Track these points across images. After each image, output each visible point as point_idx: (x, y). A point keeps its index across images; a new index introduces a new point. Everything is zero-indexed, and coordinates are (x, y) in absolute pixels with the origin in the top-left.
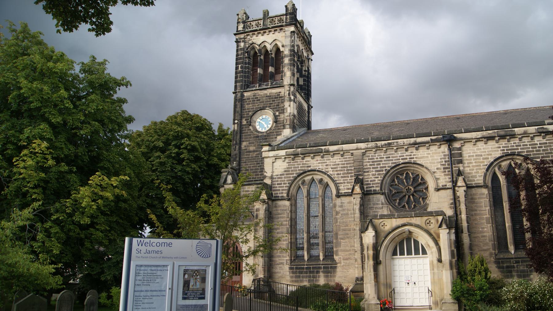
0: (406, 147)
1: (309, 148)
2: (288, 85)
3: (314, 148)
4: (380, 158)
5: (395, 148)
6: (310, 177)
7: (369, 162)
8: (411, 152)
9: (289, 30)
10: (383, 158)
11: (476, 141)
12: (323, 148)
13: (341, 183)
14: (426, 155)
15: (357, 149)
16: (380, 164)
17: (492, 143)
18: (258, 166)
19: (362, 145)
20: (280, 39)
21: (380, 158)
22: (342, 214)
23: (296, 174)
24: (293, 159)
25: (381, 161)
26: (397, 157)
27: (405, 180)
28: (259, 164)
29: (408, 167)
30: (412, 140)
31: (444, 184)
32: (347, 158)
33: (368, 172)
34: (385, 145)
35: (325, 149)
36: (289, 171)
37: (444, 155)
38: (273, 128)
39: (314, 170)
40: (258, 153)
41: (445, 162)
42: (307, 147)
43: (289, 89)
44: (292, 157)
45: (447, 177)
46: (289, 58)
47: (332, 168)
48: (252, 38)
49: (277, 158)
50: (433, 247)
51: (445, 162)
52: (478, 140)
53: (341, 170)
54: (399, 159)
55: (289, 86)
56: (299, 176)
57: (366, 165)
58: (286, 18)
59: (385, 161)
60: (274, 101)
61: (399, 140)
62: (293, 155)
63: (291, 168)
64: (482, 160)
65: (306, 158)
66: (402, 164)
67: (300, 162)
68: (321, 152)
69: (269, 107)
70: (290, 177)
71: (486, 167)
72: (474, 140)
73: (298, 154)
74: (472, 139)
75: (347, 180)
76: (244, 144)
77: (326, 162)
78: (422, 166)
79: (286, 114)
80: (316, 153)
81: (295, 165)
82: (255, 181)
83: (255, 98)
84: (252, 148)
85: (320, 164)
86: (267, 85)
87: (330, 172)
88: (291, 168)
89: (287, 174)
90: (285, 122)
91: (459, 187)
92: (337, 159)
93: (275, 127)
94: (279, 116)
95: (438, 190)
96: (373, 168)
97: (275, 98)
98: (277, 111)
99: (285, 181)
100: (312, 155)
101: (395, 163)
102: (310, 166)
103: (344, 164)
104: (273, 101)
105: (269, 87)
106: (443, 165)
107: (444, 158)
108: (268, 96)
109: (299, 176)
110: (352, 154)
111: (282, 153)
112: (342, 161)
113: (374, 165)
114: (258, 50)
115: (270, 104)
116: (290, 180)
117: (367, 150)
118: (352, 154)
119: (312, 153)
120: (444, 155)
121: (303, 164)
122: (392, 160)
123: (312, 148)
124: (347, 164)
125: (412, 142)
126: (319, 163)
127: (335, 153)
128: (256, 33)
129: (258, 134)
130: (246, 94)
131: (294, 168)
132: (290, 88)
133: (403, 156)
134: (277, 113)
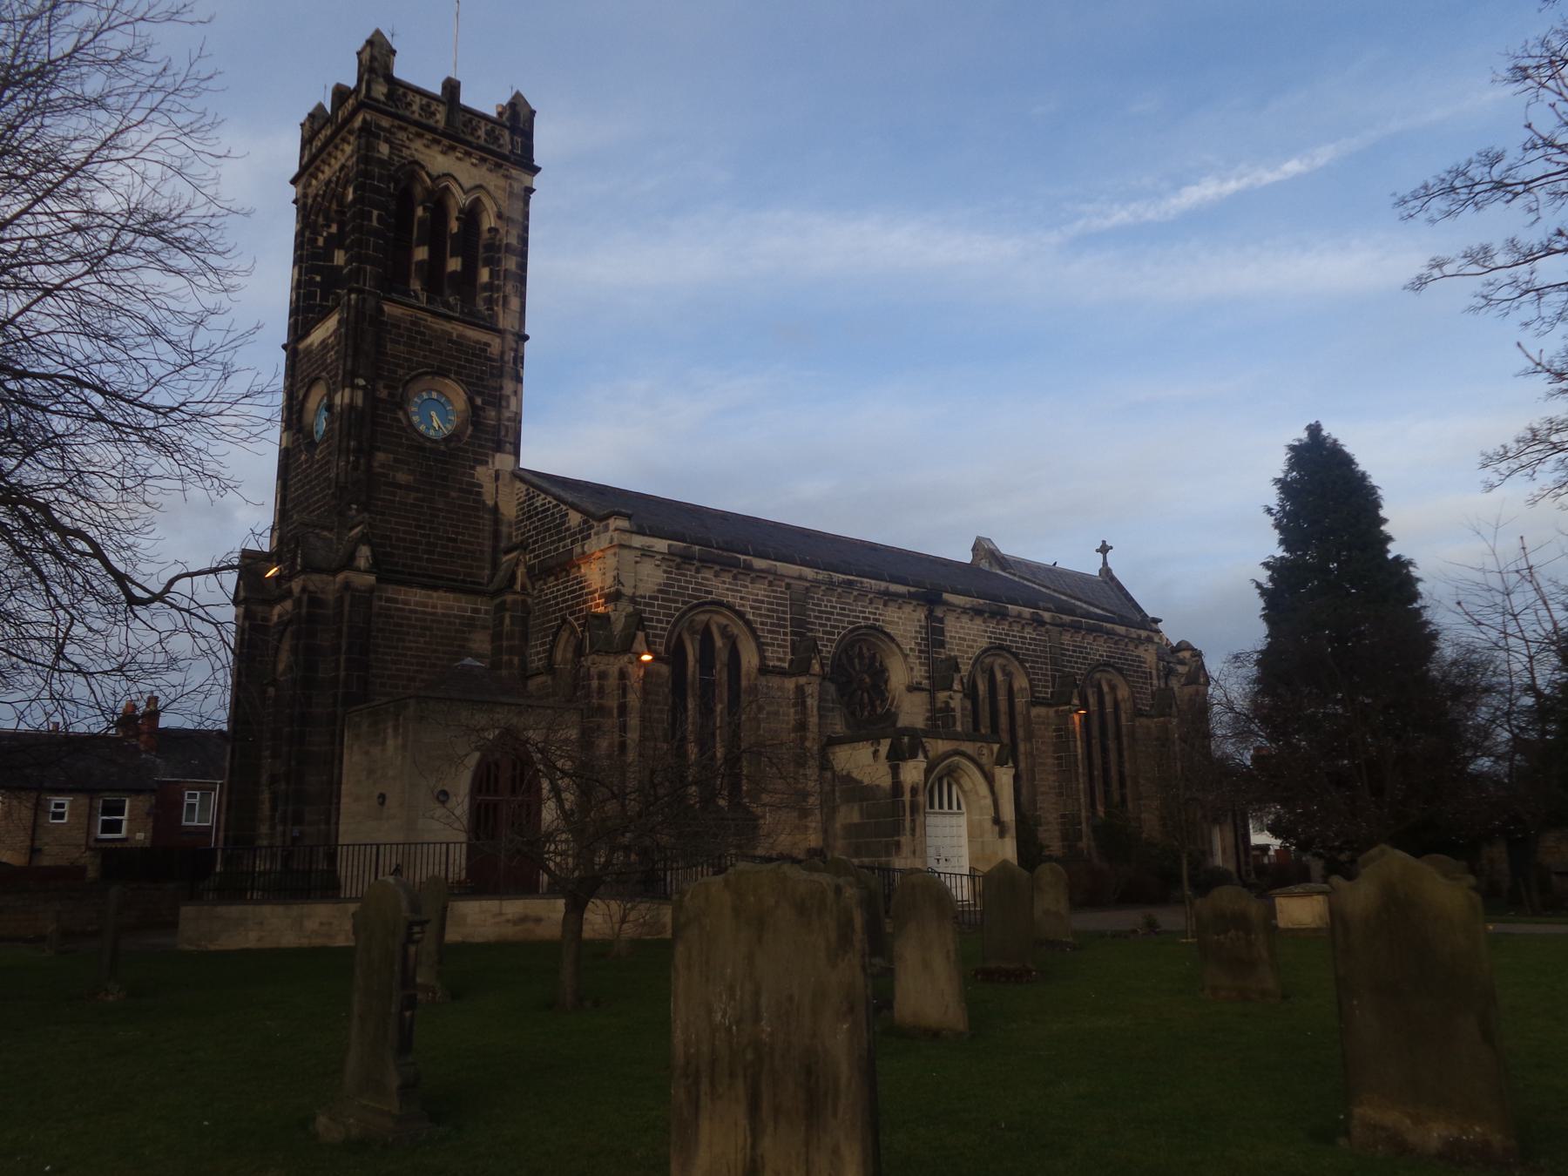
0: (870, 596)
1: (716, 551)
2: (514, 334)
3: (725, 554)
4: (831, 607)
5: (855, 593)
6: (704, 617)
7: (813, 610)
8: (877, 609)
9: (521, 182)
10: (835, 607)
11: (962, 613)
12: (742, 557)
13: (768, 644)
14: (896, 620)
15: (800, 578)
16: (828, 619)
17: (978, 621)
18: (422, 535)
19: (809, 572)
20: (491, 188)
21: (831, 607)
22: (768, 713)
23: (684, 603)
24: (678, 567)
25: (832, 613)
26: (855, 611)
27: (856, 660)
28: (423, 527)
29: (870, 635)
30: (883, 585)
31: (919, 679)
32: (776, 592)
33: (811, 630)
34: (844, 582)
35: (745, 560)
36: (667, 592)
37: (921, 627)
38: (466, 439)
39: (721, 604)
40: (421, 495)
41: (922, 639)
42: (713, 547)
43: (514, 346)
44: (678, 560)
45: (923, 668)
46: (519, 259)
47: (751, 608)
48: (413, 146)
49: (646, 553)
50: (985, 797)
51: (922, 639)
52: (965, 611)
53: (768, 617)
54: (858, 617)
55: (516, 338)
56: (691, 609)
57: (809, 616)
58: (512, 140)
59: (838, 614)
60: (470, 362)
61: (865, 580)
62: (681, 556)
63: (672, 586)
64: (965, 648)
65: (705, 570)
66: (866, 627)
67: (692, 576)
68: (736, 567)
69: (456, 373)
70: (670, 608)
71: (971, 662)
72: (959, 610)
73: (693, 558)
74: (959, 607)
75: (776, 639)
76: (381, 456)
77: (740, 592)
78: (892, 639)
79: (507, 414)
80: (728, 565)
81: (680, 581)
82: (410, 574)
83: (417, 333)
84: (402, 477)
85: (730, 593)
86: (447, 305)
87: (751, 617)
88: (672, 586)
89: (663, 599)
90: (503, 433)
91: (955, 691)
92: (760, 589)
93: (471, 436)
94: (483, 409)
95: (912, 688)
96: (821, 625)
97: (474, 355)
98: (480, 394)
99: (658, 614)
100: (717, 568)
101: (853, 623)
102: (711, 593)
103: (772, 603)
104: (467, 360)
105: (457, 315)
106: (919, 644)
107: (920, 633)
108: (454, 342)
109: (691, 609)
110: (788, 586)
111: (661, 545)
112: (769, 597)
113: (821, 618)
114: (426, 189)
115: (459, 366)
116: (672, 616)
117: (816, 583)
118: (788, 586)
119: (719, 564)
120: (921, 627)
121: (696, 583)
122: (848, 616)
123: (720, 552)
124: (778, 604)
125: (882, 589)
126: (728, 589)
127: (761, 575)
128: (429, 136)
129: (421, 440)
130: (387, 308)
131: (679, 587)
132: (517, 343)
133: (864, 612)
134: (479, 401)
